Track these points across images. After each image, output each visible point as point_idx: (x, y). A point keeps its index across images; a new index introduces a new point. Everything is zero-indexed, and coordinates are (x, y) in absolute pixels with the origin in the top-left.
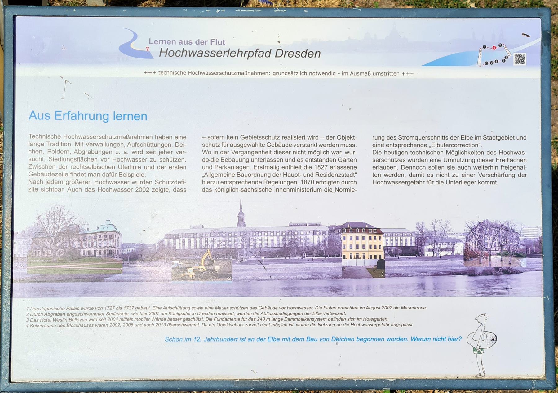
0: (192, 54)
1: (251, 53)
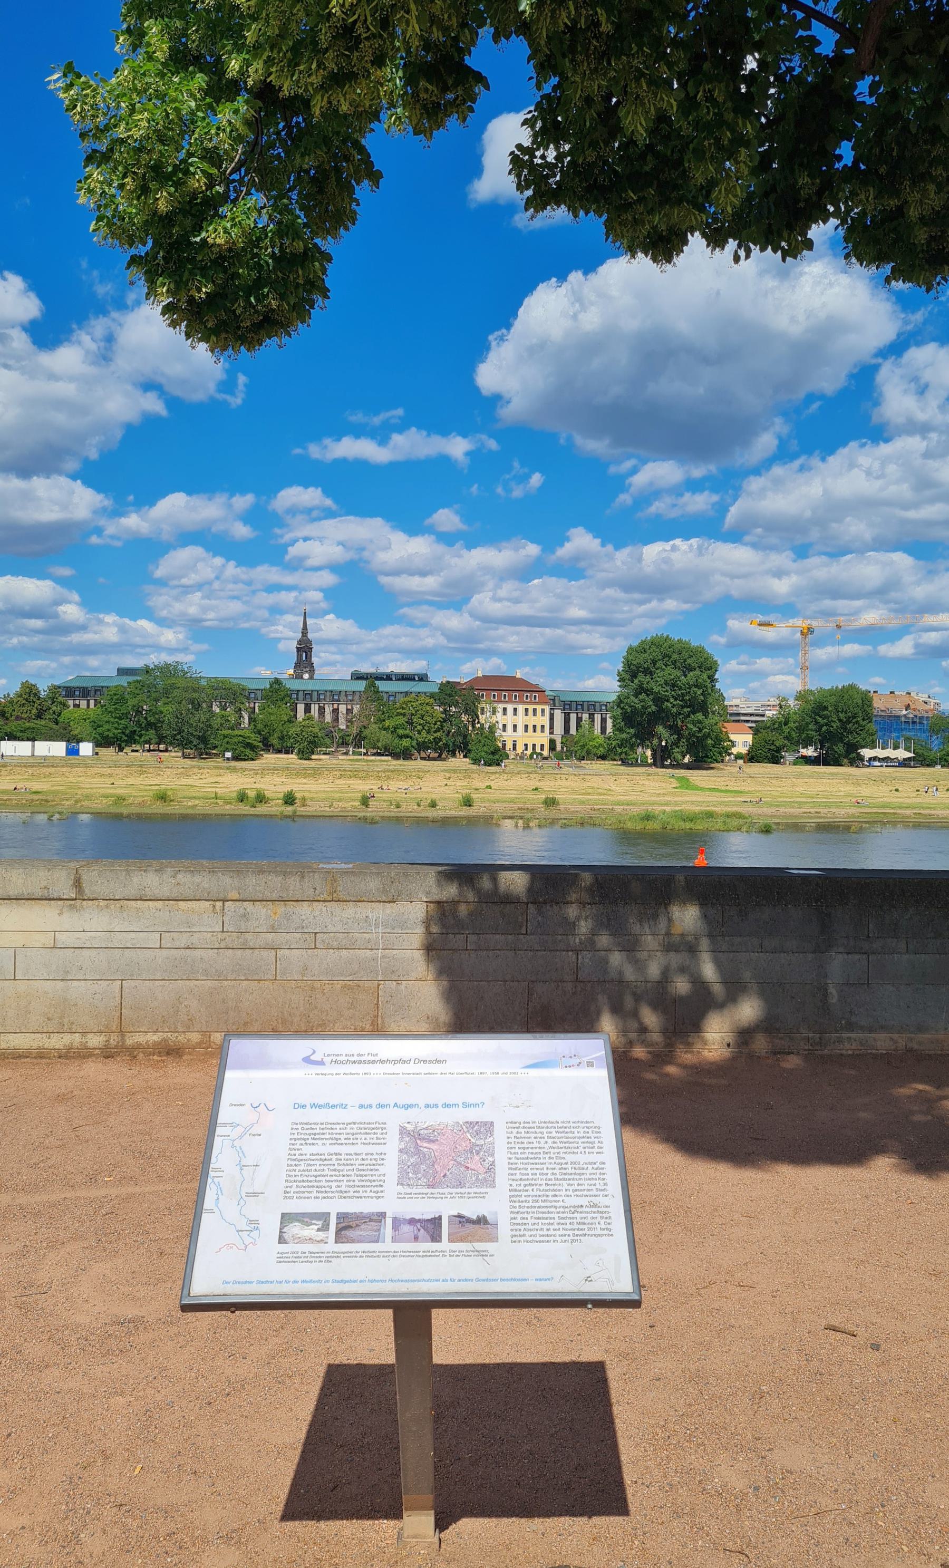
0: (354, 1062)
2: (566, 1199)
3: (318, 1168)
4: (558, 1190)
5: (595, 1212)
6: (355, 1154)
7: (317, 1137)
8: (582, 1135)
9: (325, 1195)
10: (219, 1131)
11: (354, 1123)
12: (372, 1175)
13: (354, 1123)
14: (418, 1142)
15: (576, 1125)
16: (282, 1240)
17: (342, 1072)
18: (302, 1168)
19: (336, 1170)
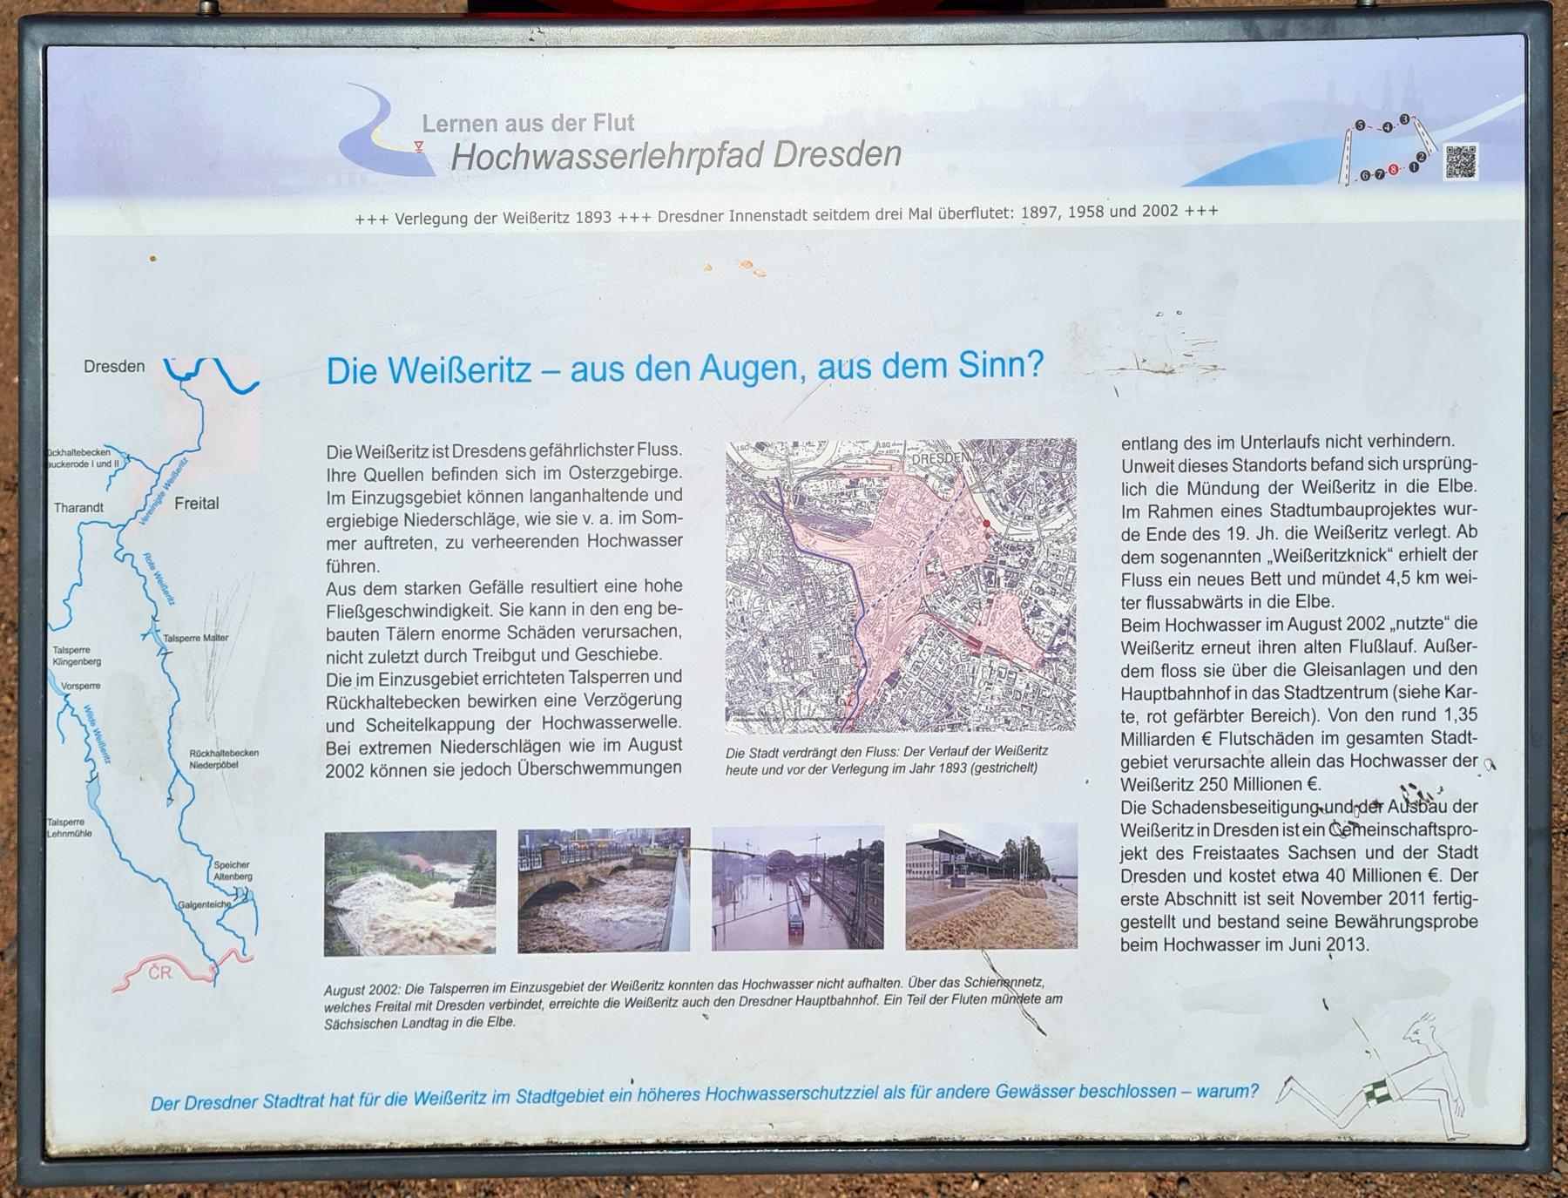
0: (543, 160)
1: (708, 155)
2: (1325, 776)
3: (440, 645)
4: (1297, 739)
5: (1424, 831)
6: (570, 586)
7: (428, 510)
8: (1401, 498)
9: (474, 759)
10: (63, 485)
11: (561, 451)
12: (636, 678)
13: (561, 451)
14: (799, 530)
15: (1384, 453)
16: (336, 943)
17: (498, 208)
18: (382, 645)
19: (503, 656)
